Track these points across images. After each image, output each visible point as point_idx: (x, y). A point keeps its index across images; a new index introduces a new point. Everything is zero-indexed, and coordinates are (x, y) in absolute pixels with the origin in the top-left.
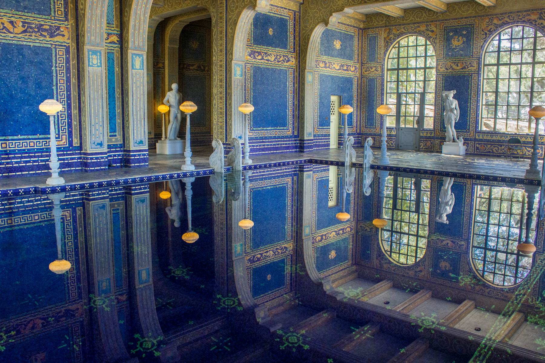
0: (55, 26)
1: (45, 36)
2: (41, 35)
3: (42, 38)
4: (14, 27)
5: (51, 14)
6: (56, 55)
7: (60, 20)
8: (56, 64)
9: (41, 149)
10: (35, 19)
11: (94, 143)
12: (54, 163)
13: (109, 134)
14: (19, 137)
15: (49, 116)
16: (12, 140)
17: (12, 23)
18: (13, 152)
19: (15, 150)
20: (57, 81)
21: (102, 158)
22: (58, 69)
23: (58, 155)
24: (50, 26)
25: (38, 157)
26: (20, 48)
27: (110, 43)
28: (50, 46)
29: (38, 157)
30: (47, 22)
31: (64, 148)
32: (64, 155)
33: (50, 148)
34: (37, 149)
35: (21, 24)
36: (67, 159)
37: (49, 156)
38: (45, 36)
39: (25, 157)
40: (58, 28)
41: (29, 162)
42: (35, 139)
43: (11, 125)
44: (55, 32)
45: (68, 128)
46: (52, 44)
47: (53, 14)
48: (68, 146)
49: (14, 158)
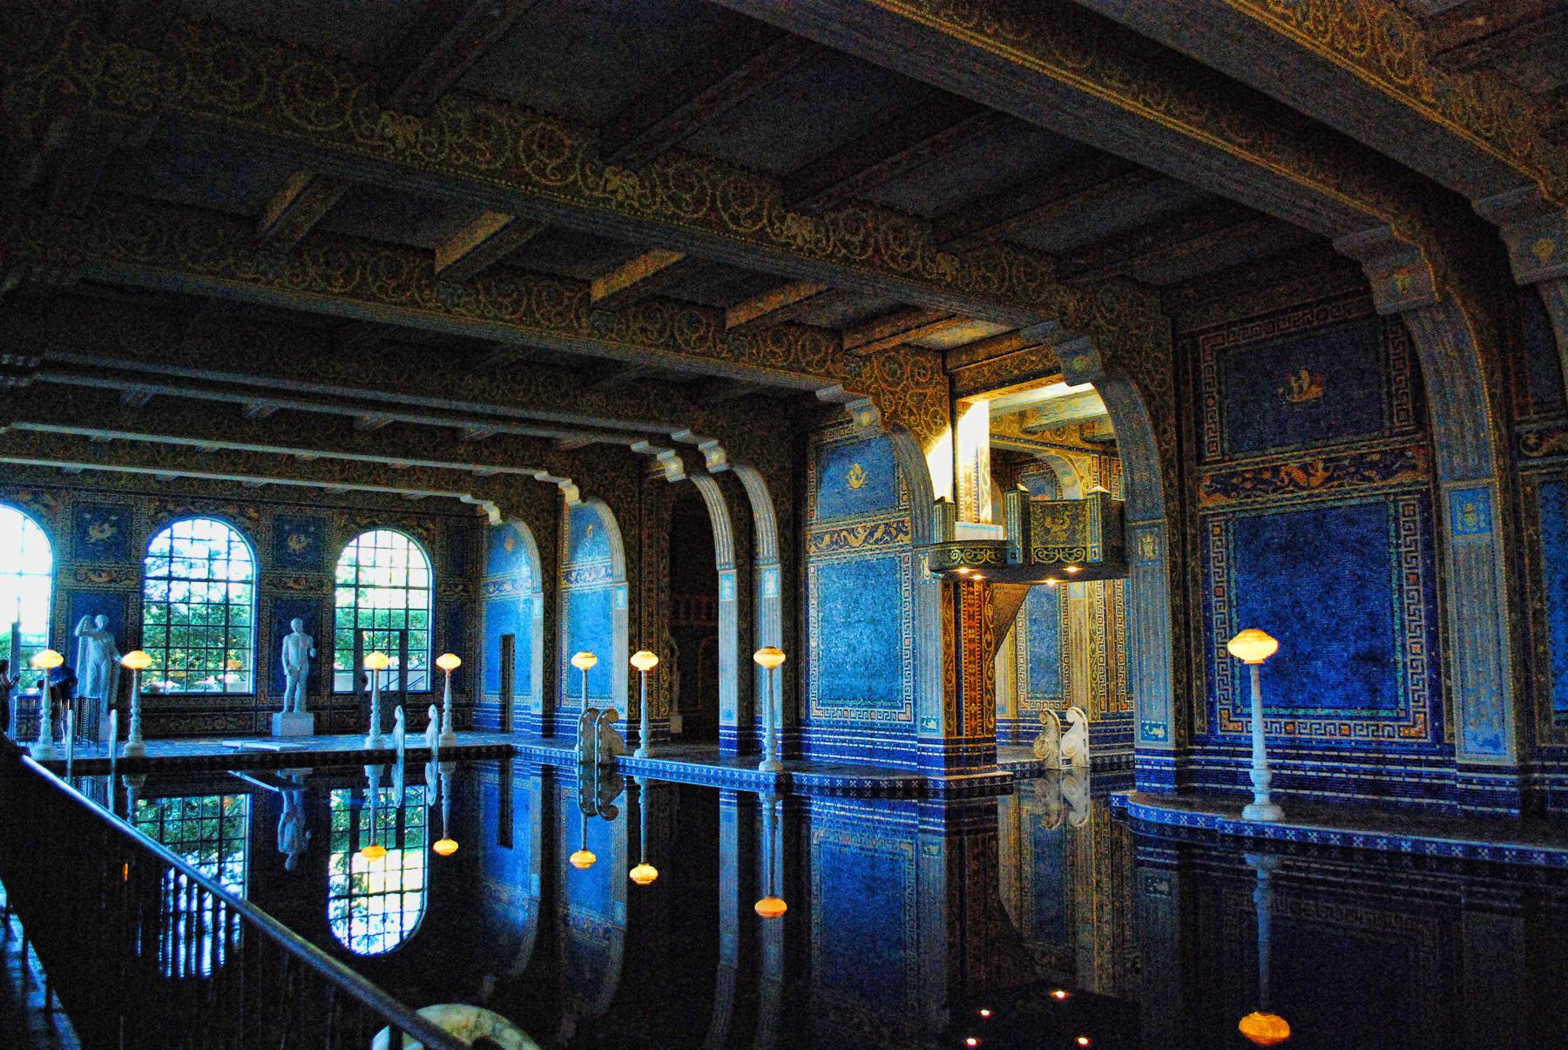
0: (1392, 451)
1: (1370, 480)
2: (1364, 478)
3: (1365, 485)
4: (1309, 475)
5: (1382, 425)
6: (1396, 519)
7: (1403, 434)
8: (1398, 537)
9: (1364, 743)
10: (1344, 448)
11: (1475, 739)
12: (1259, 771)
13: (1554, 718)
14: (1320, 712)
15: (1248, 667)
16: (1306, 716)
17: (1305, 468)
18: (1307, 744)
19: (1310, 741)
20: (1400, 578)
21: (1500, 783)
22: (1403, 549)
23: (1271, 755)
24: (1381, 452)
25: (1358, 760)
26: (1320, 516)
27: (1548, 454)
28: (1382, 498)
29: (1358, 760)
30: (1374, 448)
31: (1419, 745)
32: (1419, 763)
33: (1251, 739)
34: (1357, 742)
35: (1321, 465)
36: (1429, 775)
37: (1250, 754)
38: (1370, 480)
39: (1331, 759)
40: (1402, 453)
41: (1339, 770)
42: (1351, 718)
43: (1304, 685)
44: (1393, 463)
45: (1432, 696)
46: (1387, 495)
47: (1387, 424)
48: (1429, 740)
49: (1309, 757)
